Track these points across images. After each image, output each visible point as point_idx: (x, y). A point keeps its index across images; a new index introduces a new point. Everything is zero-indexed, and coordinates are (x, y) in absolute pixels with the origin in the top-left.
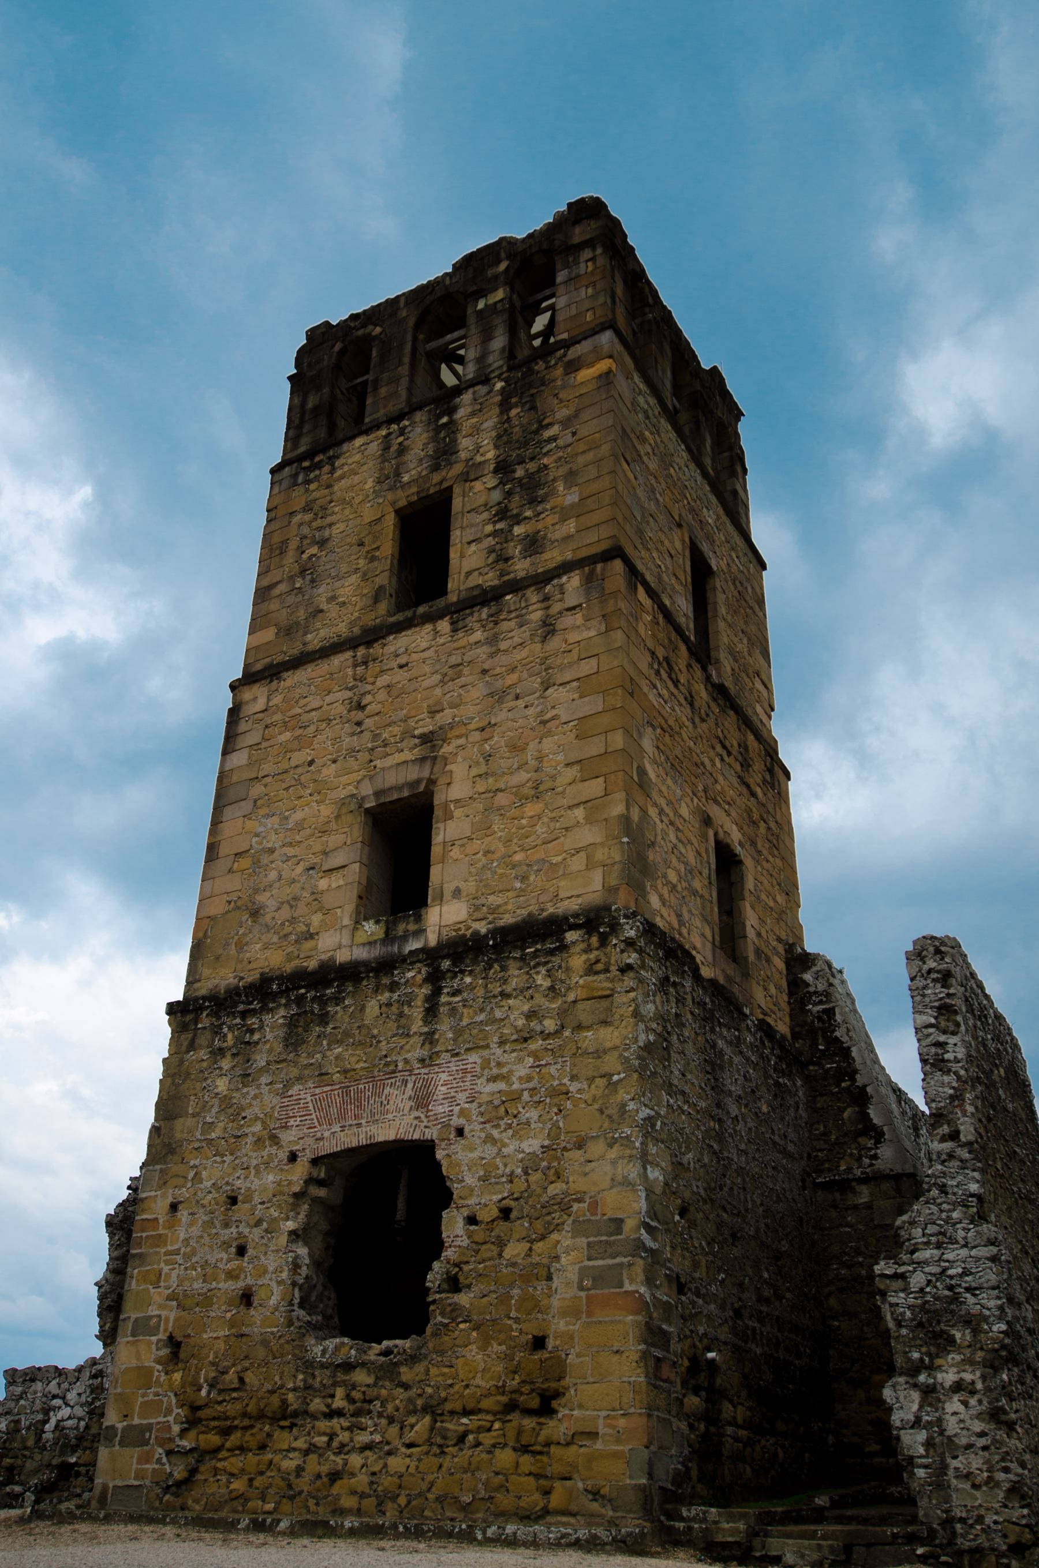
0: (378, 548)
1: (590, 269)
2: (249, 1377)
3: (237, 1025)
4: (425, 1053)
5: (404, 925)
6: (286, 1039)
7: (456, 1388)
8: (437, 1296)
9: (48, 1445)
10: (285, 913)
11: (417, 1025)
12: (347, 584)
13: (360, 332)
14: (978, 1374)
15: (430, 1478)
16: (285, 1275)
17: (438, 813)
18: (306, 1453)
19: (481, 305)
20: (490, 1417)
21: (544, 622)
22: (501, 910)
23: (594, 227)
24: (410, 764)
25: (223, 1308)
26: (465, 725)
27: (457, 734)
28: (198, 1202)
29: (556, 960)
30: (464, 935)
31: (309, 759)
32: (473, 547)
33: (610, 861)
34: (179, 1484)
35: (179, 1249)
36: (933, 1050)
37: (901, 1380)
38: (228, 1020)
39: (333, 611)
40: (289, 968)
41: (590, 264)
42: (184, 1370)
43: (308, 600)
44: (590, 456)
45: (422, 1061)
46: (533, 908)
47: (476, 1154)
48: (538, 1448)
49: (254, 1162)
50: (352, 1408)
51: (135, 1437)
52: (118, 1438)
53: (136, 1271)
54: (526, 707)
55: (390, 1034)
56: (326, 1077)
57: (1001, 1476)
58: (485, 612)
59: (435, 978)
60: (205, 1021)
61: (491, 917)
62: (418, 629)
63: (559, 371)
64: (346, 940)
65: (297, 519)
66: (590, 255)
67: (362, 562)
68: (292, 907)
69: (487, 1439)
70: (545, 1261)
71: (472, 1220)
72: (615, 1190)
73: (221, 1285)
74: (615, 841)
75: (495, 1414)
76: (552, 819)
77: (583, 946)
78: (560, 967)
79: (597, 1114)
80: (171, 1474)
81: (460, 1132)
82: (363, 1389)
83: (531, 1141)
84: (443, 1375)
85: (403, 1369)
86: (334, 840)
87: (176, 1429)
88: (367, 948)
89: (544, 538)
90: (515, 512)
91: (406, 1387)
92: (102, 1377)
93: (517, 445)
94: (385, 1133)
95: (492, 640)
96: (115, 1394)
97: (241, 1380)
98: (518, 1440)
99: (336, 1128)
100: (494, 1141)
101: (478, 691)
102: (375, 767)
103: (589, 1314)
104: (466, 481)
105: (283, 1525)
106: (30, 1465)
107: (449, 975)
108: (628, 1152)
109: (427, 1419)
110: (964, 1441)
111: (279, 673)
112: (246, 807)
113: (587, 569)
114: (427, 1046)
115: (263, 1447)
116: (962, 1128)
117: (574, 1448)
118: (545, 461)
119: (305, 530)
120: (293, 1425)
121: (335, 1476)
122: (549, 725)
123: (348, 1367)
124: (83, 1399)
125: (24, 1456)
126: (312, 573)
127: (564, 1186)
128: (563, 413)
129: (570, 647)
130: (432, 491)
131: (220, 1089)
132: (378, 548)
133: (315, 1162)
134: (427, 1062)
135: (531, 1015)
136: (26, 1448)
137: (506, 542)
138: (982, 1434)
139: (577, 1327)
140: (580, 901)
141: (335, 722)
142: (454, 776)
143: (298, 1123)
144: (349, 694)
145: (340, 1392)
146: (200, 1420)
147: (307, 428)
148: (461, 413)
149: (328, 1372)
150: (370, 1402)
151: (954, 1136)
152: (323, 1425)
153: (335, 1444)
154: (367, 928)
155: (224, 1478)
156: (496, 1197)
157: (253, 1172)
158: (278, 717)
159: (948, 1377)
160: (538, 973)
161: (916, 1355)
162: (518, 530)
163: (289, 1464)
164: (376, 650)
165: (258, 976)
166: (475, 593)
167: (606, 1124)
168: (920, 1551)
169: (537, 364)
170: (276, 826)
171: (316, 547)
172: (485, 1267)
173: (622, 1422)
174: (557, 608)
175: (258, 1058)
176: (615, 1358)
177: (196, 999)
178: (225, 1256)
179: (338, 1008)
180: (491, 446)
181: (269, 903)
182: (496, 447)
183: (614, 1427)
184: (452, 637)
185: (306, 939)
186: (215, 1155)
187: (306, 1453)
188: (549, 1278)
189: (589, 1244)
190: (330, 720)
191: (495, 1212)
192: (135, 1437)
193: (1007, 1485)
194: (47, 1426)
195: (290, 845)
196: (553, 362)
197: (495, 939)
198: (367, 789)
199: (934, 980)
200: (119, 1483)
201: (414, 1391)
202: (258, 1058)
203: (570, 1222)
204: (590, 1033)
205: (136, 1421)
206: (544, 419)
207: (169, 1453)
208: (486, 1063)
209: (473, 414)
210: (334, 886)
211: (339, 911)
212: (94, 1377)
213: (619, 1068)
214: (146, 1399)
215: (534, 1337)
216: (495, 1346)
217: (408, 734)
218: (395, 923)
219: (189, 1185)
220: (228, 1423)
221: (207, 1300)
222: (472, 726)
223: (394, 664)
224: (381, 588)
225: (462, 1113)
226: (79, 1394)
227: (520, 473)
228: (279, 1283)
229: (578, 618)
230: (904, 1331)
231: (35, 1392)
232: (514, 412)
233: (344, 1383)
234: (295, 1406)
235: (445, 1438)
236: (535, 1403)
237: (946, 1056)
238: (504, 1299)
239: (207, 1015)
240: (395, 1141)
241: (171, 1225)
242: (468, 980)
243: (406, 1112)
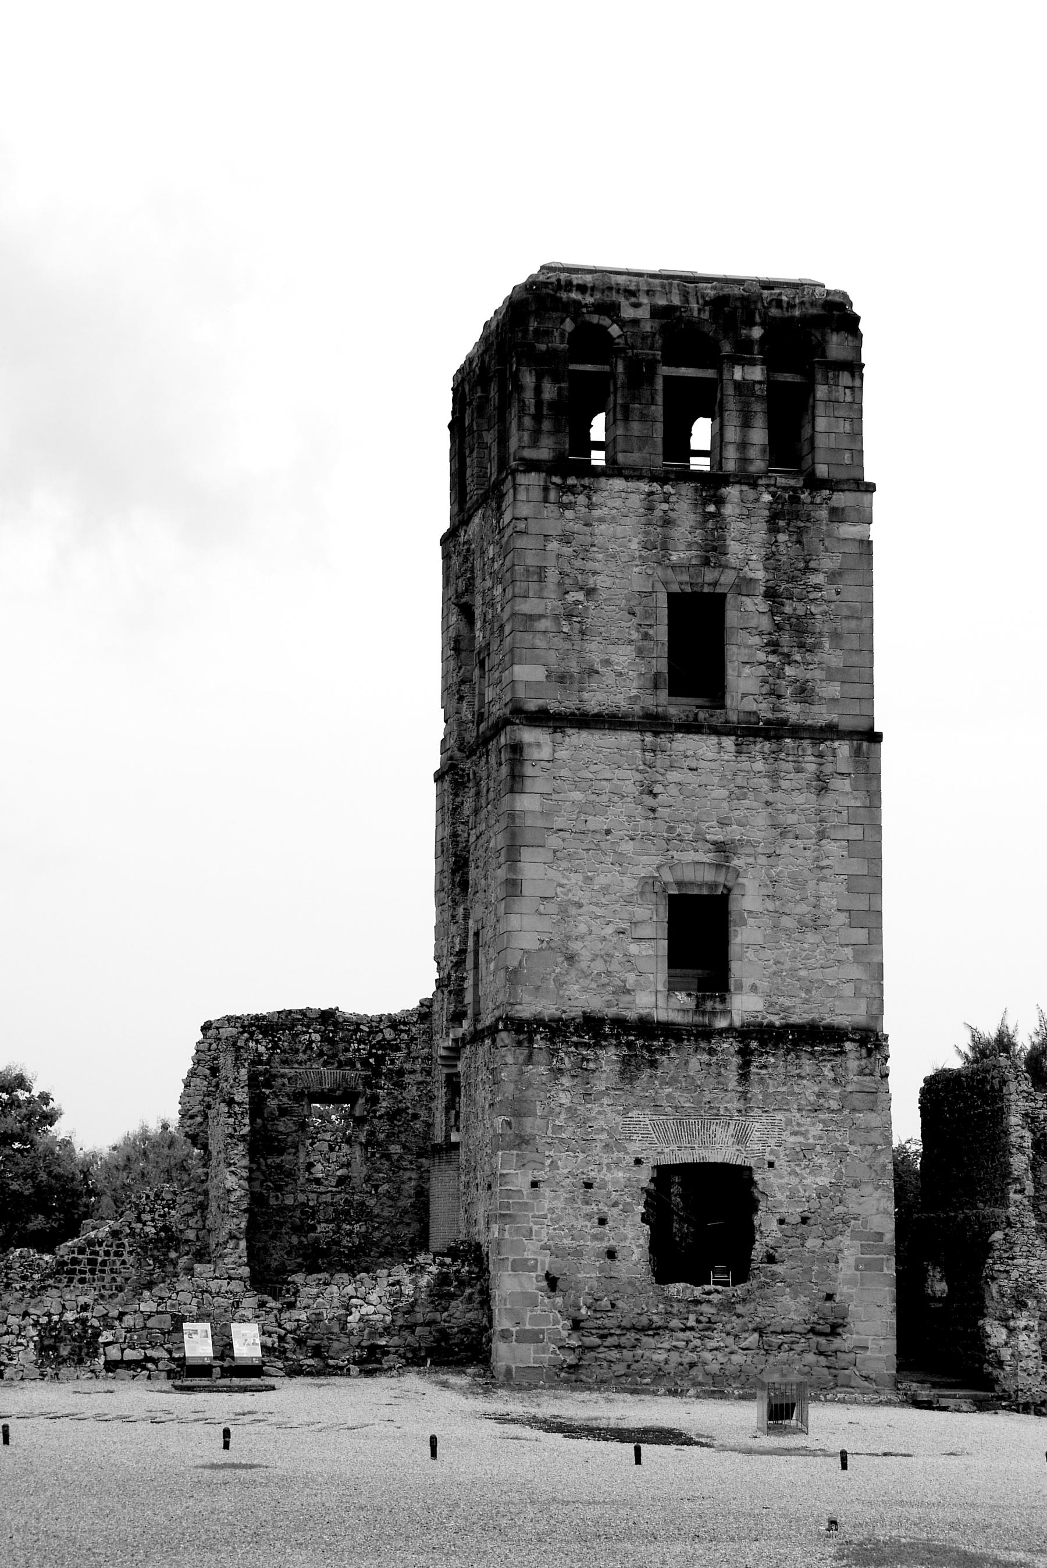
0: (651, 626)
1: (849, 399)
2: (620, 1304)
3: (572, 1052)
4: (740, 1105)
5: (712, 1003)
6: (622, 1074)
7: (777, 1319)
8: (761, 1265)
9: (355, 1331)
10: (599, 966)
11: (732, 1084)
12: (620, 652)
13: (595, 319)
14: (1037, 1322)
15: (762, 1367)
16: (641, 1242)
17: (733, 917)
18: (669, 1350)
19: (738, 374)
20: (798, 1336)
21: (818, 776)
22: (791, 1011)
23: (850, 344)
24: (707, 866)
25: (593, 1258)
26: (754, 846)
27: (746, 852)
28: (558, 1183)
29: (838, 1060)
30: (761, 1025)
31: (605, 827)
32: (747, 670)
33: (872, 996)
34: (570, 1367)
35: (546, 1215)
36: (1019, 1140)
37: (996, 1322)
38: (564, 1047)
39: (610, 678)
40: (612, 1012)
41: (847, 391)
42: (564, 1297)
43: (580, 652)
44: (853, 624)
45: (740, 1111)
46: (815, 1015)
47: (782, 1181)
48: (830, 1353)
49: (605, 1161)
50: (701, 1326)
51: (533, 1337)
52: (514, 1337)
53: (507, 1226)
54: (805, 849)
55: (712, 1087)
56: (659, 1108)
57: (1041, 1370)
58: (767, 746)
59: (745, 1053)
60: (539, 1043)
61: (782, 1014)
62: (704, 737)
63: (824, 514)
64: (661, 1002)
65: (553, 546)
66: (850, 385)
67: (635, 636)
68: (606, 961)
69: (798, 1348)
70: (834, 1252)
71: (781, 1222)
72: (879, 1216)
73: (589, 1243)
74: (876, 982)
75: (801, 1334)
76: (829, 950)
77: (857, 1055)
78: (841, 1066)
79: (868, 1169)
80: (565, 1361)
81: (771, 1165)
82: (709, 1316)
83: (822, 1178)
84: (768, 1311)
85: (737, 1306)
86: (642, 912)
87: (565, 1333)
88: (681, 1014)
89: (813, 690)
90: (786, 650)
91: (739, 1316)
92: (400, 1286)
93: (785, 577)
94: (715, 1157)
95: (774, 776)
96: (506, 1309)
97: (613, 1306)
98: (817, 1348)
99: (674, 1147)
100: (797, 1174)
101: (761, 819)
102: (673, 858)
103: (862, 1285)
104: (739, 594)
105: (692, 1392)
106: (336, 1345)
107: (756, 1052)
108: (887, 1194)
109: (756, 1335)
110: (1026, 1354)
111: (564, 727)
112: (544, 855)
113: (855, 742)
114: (742, 1101)
115: (634, 1347)
116: (1027, 1187)
117: (852, 1355)
118: (814, 609)
119: (568, 569)
120: (658, 1334)
121: (692, 1365)
122: (824, 871)
123: (697, 1302)
124: (385, 1300)
125: (331, 1339)
126: (579, 622)
127: (846, 1209)
128: (828, 563)
129: (839, 809)
130: (706, 589)
131: (563, 1101)
132: (651, 626)
133: (654, 1167)
134: (744, 1112)
135: (820, 1095)
136: (332, 1333)
137: (779, 678)
138: (1036, 1351)
139: (854, 1291)
140: (849, 1019)
141: (629, 800)
142: (747, 890)
143: (640, 1138)
144: (639, 777)
145: (692, 1318)
146: (583, 1328)
147: (546, 425)
148: (728, 510)
149: (682, 1304)
150: (715, 1323)
151: (1022, 1191)
152: (681, 1335)
153: (691, 1345)
154: (679, 997)
155: (605, 1364)
156: (799, 1210)
157: (605, 1168)
158: (563, 773)
159: (1022, 1323)
160: (824, 1066)
161: (1010, 1312)
162: (789, 671)
163: (660, 1357)
164: (663, 740)
165: (581, 1013)
166: (753, 719)
167: (873, 1176)
168: (1004, 1404)
169: (803, 493)
170: (580, 883)
171: (582, 593)
172: (793, 1252)
173: (882, 1343)
174: (828, 769)
175: (597, 1082)
176: (878, 1309)
177: (529, 1022)
178: (589, 1224)
179: (664, 1058)
180: (760, 566)
181: (583, 952)
182: (766, 569)
183: (877, 1345)
184: (736, 757)
185: (623, 992)
186: (567, 1151)
187: (669, 1350)
188: (837, 1262)
189: (862, 1245)
190: (624, 796)
191: (799, 1220)
192: (533, 1337)
193: (1043, 1375)
194: (350, 1318)
195: (597, 904)
196: (818, 500)
197: (793, 1036)
198: (667, 876)
199: (1024, 1097)
200: (518, 1365)
201: (746, 1319)
202: (597, 1082)
203: (849, 1230)
204: (861, 1115)
205: (528, 1327)
206: (810, 560)
207: (560, 1348)
208: (789, 1122)
209: (741, 517)
210: (644, 953)
211: (651, 975)
212: (393, 1285)
213: (882, 1142)
214: (534, 1313)
215: (827, 1294)
216: (802, 1297)
217: (699, 837)
218: (704, 998)
219: (547, 1169)
220: (606, 1331)
221: (578, 1253)
222: (759, 850)
223: (685, 765)
224: (657, 674)
225: (772, 1152)
226: (380, 1297)
227: (788, 610)
228: (639, 1246)
229: (845, 785)
230: (1005, 1300)
231: (331, 1293)
232: (782, 537)
233: (695, 1312)
234: (660, 1324)
235: (770, 1346)
236: (827, 1329)
237: (1025, 1144)
238: (807, 1272)
239: (542, 1039)
240: (721, 1163)
241: (536, 1198)
242: (772, 1060)
243: (730, 1144)
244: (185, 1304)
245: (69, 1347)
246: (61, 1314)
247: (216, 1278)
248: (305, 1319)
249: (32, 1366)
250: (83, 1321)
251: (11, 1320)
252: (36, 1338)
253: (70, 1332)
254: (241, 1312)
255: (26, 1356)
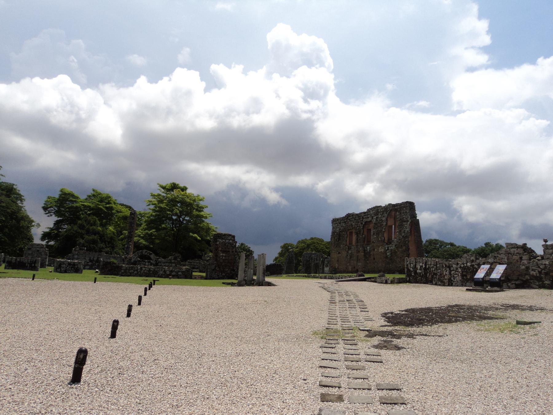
244: (503, 259)
245: (470, 276)
246: (466, 264)
247: (513, 248)
248: (548, 264)
249: (459, 282)
250: (472, 266)
251: (454, 266)
252: (461, 272)
253: (469, 270)
254: (523, 261)
255: (459, 278)
